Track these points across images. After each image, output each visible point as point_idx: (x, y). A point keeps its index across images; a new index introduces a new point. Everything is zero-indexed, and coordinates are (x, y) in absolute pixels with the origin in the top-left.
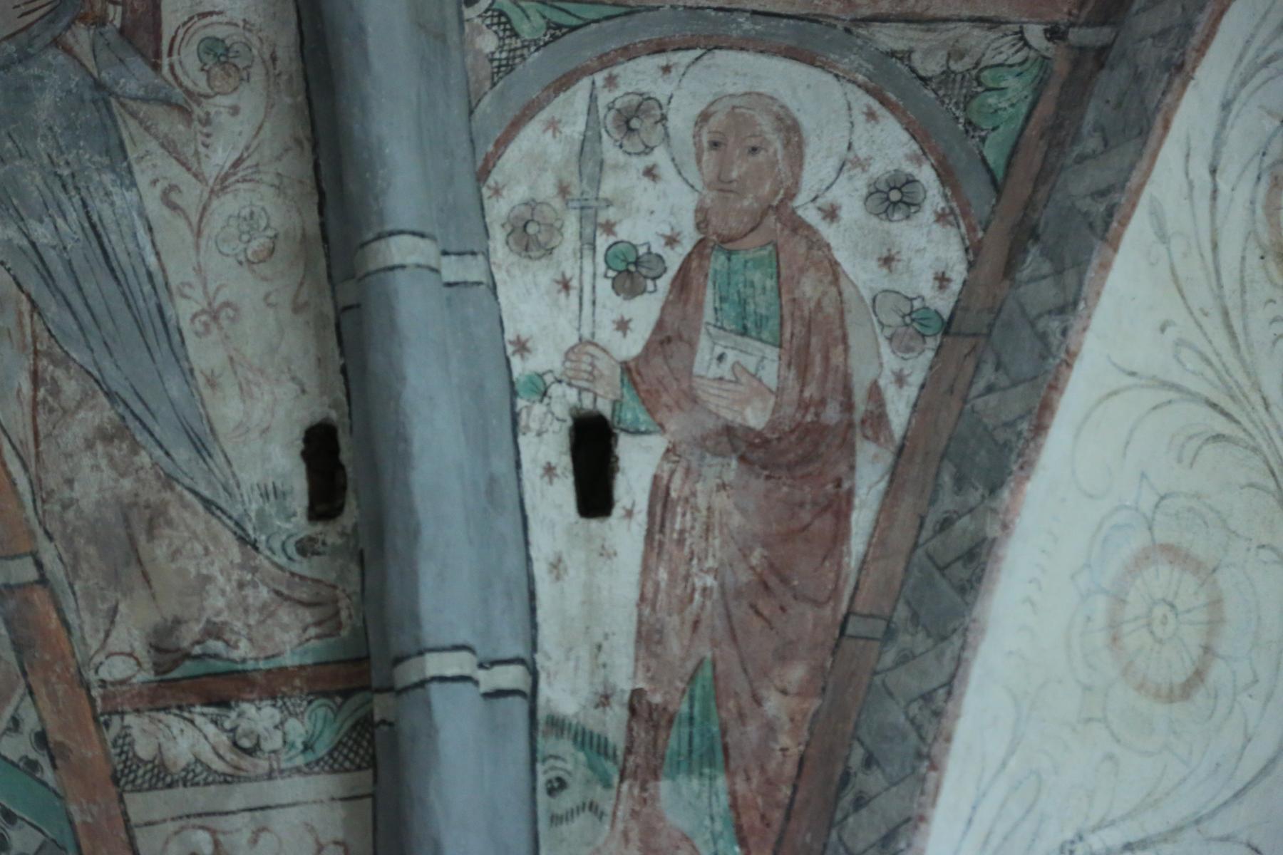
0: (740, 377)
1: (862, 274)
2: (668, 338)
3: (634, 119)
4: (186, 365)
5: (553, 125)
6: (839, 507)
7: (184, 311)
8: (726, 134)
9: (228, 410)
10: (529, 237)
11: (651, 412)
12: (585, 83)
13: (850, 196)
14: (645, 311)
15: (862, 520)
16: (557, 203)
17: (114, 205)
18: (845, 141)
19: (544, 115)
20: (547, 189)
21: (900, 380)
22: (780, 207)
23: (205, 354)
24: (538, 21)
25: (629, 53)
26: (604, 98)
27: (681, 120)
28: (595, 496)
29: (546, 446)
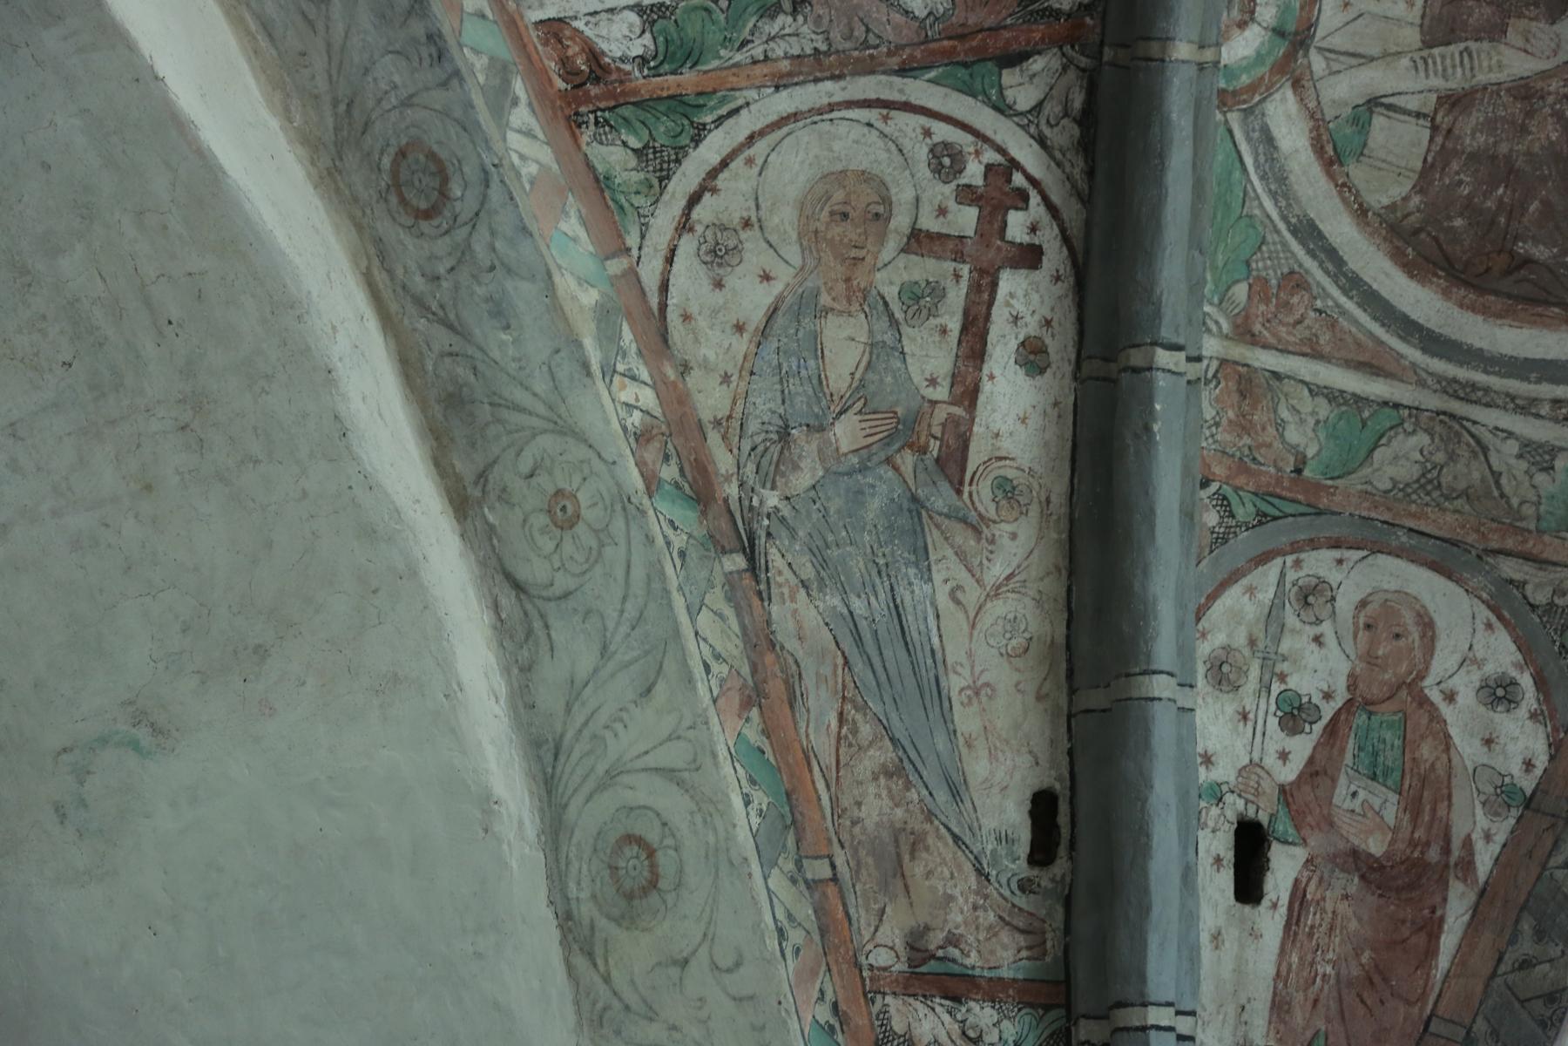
0: (1368, 812)
1: (1468, 749)
2: (1317, 772)
3: (1311, 595)
4: (951, 727)
5: (1251, 590)
6: (1432, 928)
7: (955, 684)
8: (1380, 621)
9: (978, 768)
10: (1223, 674)
11: (1297, 828)
12: (1279, 561)
13: (1466, 686)
14: (1302, 747)
15: (1449, 941)
16: (1247, 652)
17: (914, 593)
18: (1468, 645)
19: (1245, 581)
20: (1240, 640)
21: (1488, 837)
22: (1411, 685)
23: (966, 720)
24: (1251, 509)
25: (1314, 544)
26: (1291, 576)
27: (1346, 603)
28: (1248, 888)
29: (1217, 843)
